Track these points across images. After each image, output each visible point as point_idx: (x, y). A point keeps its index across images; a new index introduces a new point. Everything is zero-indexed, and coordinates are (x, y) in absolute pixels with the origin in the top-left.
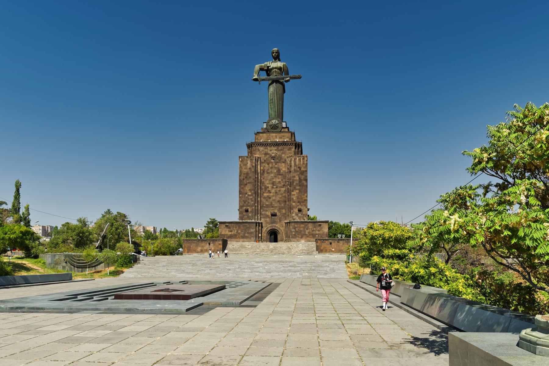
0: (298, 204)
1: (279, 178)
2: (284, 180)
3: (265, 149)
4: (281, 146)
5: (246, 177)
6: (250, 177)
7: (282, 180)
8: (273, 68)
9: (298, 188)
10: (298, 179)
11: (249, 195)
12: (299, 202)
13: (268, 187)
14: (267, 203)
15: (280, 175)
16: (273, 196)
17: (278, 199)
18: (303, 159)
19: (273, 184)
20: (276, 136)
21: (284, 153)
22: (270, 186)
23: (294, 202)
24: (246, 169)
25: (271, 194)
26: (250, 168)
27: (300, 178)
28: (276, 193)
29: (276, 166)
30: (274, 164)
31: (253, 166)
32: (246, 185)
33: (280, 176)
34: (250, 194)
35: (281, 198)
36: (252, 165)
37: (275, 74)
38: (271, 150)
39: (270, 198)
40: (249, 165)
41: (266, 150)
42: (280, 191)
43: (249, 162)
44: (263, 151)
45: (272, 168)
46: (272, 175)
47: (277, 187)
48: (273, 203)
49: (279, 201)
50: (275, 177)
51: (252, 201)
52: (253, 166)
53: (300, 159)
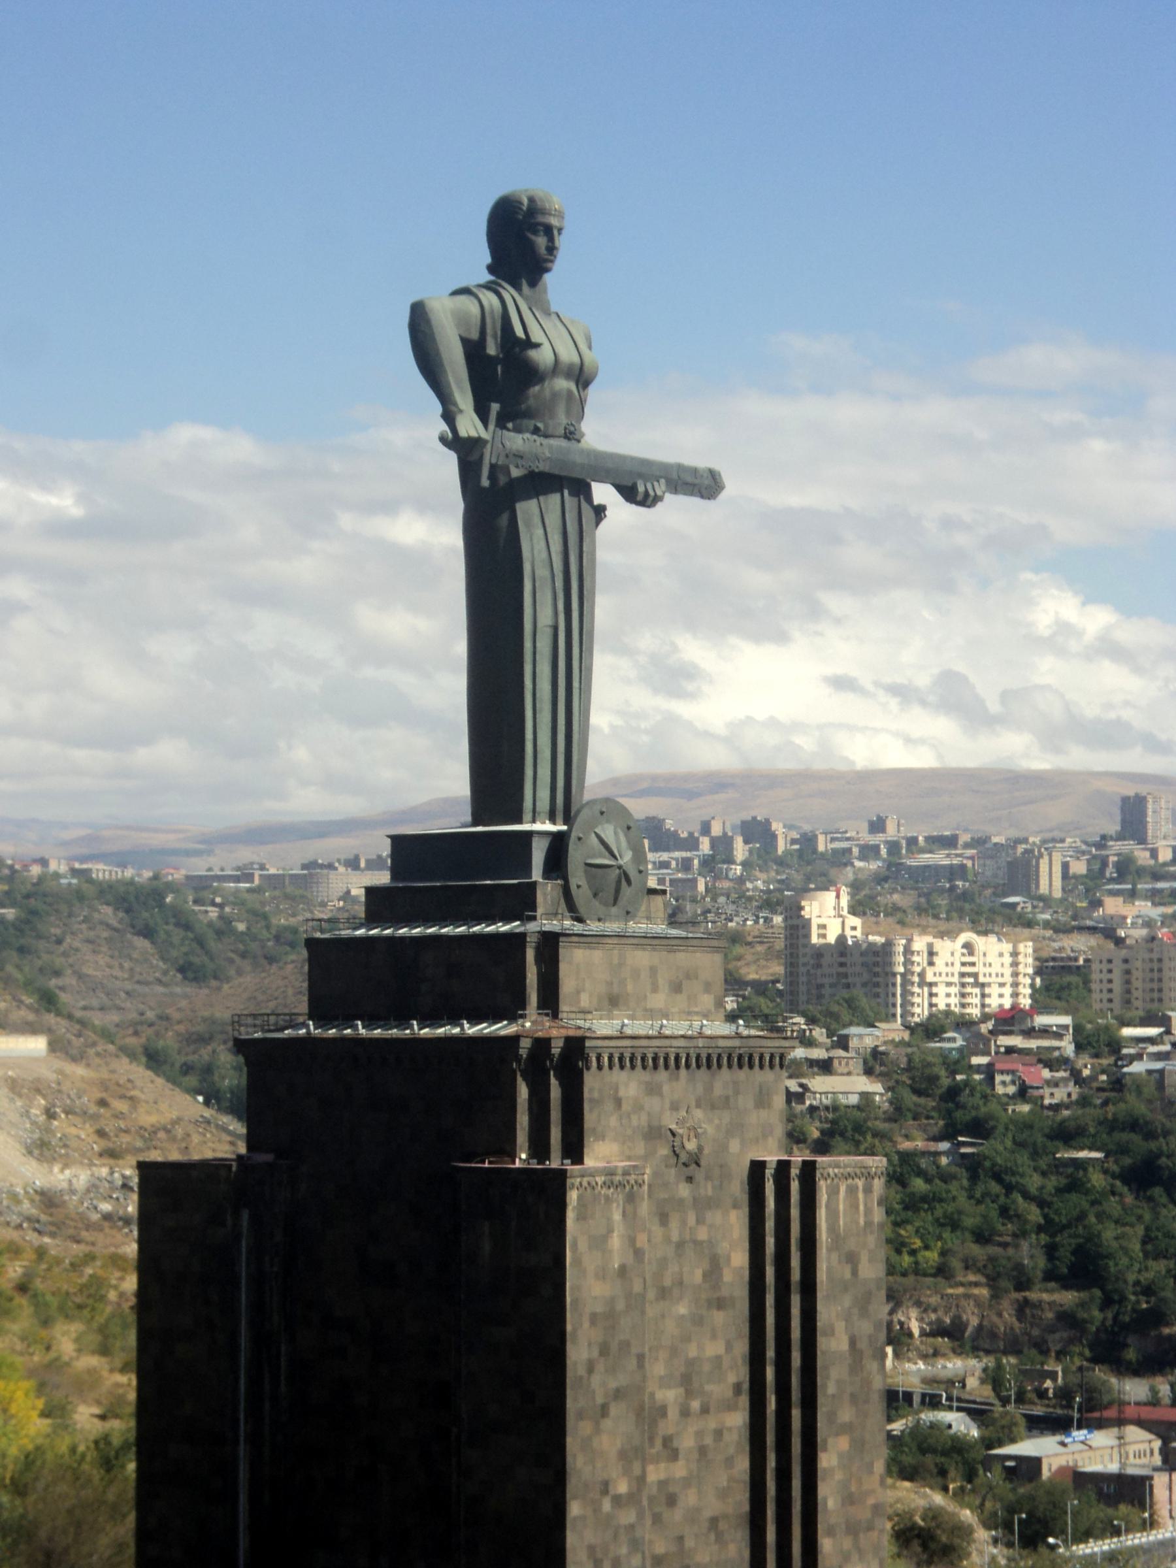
0: (847, 1543)
1: (714, 1337)
2: (742, 1347)
3: (653, 1090)
4: (725, 1072)
5: (604, 1351)
6: (625, 1345)
7: (729, 1347)
8: (557, 368)
9: (846, 1415)
10: (844, 1346)
11: (617, 1500)
12: (853, 1529)
13: (662, 1411)
14: (660, 1548)
15: (721, 1304)
16: (687, 1482)
17: (713, 1506)
18: (868, 1190)
19: (687, 1381)
20: (653, 970)
21: (736, 1128)
22: (670, 1396)
23: (831, 1533)
24: (602, 1275)
25: (679, 1470)
26: (623, 1271)
27: (853, 1342)
28: (702, 1450)
29: (702, 1234)
30: (691, 1219)
31: (638, 1253)
32: (604, 1411)
33: (719, 1318)
34: (622, 1488)
35: (723, 1494)
36: (632, 1241)
37: (562, 419)
38: (675, 1107)
39: (671, 1501)
40: (616, 1242)
41: (653, 1104)
42: (719, 1434)
43: (617, 1216)
44: (638, 1108)
45: (680, 1245)
46: (682, 1309)
47: (705, 1410)
48: (689, 1543)
49: (714, 1521)
50: (698, 1321)
51: (636, 1545)
52: (638, 1253)
53: (852, 1190)
